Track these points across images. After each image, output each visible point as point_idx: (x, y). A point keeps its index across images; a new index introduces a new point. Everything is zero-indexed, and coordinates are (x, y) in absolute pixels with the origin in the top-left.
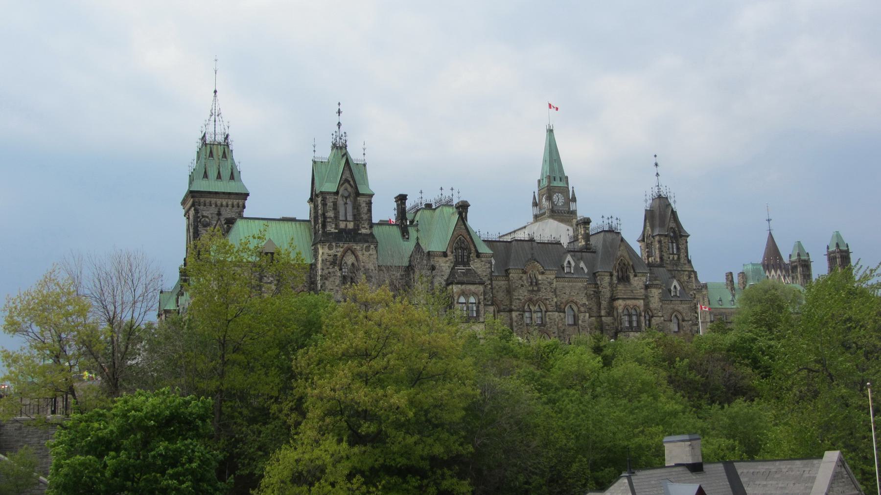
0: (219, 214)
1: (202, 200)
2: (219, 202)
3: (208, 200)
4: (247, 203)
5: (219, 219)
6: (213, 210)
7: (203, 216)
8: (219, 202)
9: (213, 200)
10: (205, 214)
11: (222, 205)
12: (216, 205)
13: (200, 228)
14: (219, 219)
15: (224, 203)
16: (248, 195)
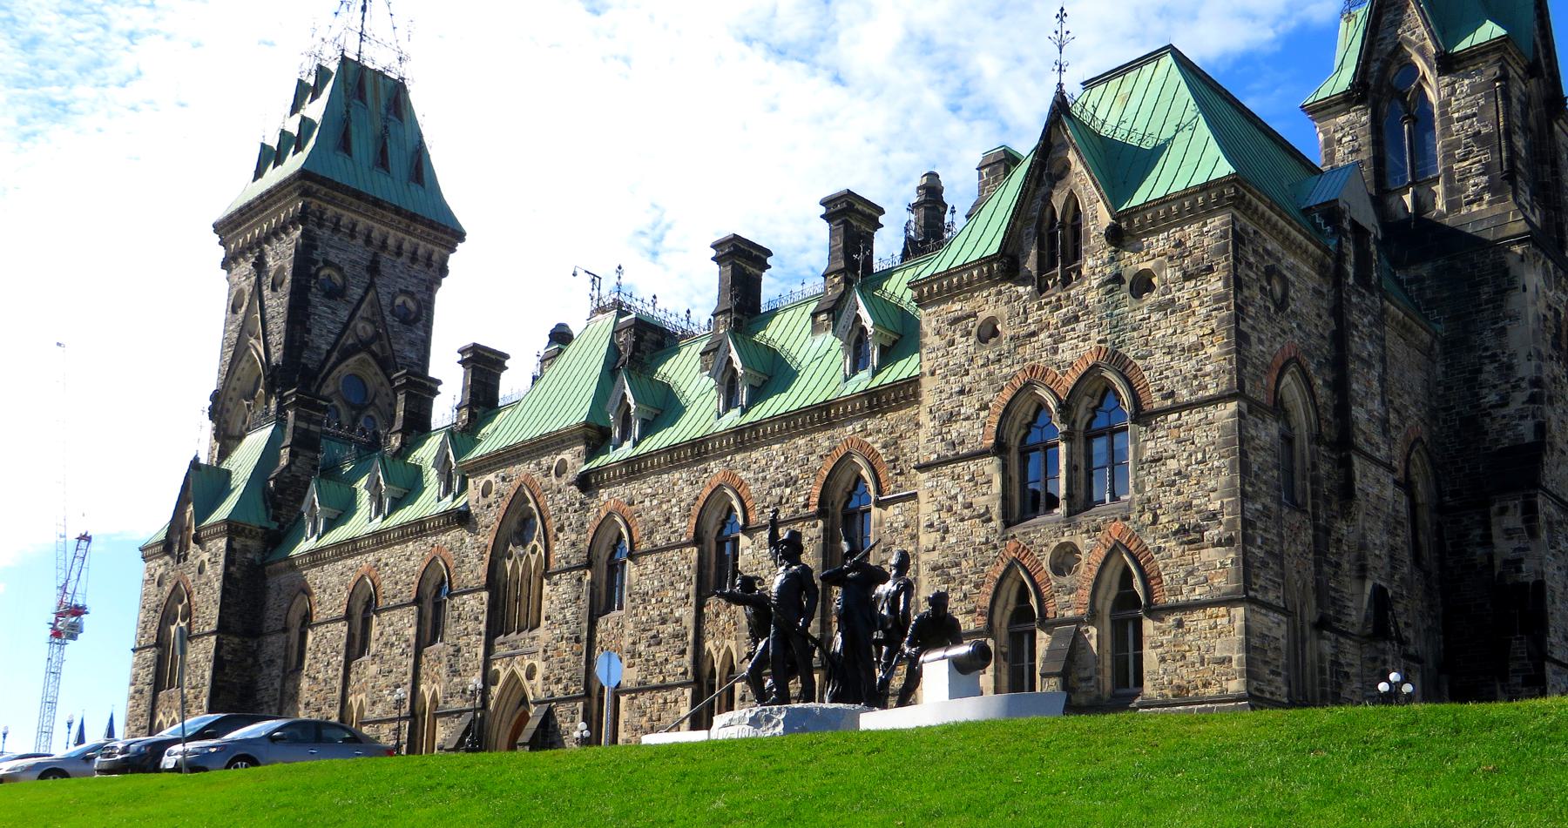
0: (374, 268)
1: (331, 210)
2: (378, 230)
3: (347, 217)
4: (453, 261)
5: (371, 286)
6: (358, 252)
7: (327, 263)
8: (378, 230)
9: (363, 223)
10: (333, 256)
11: (384, 246)
12: (368, 240)
13: (315, 298)
14: (371, 286)
15: (391, 242)
16: (460, 235)
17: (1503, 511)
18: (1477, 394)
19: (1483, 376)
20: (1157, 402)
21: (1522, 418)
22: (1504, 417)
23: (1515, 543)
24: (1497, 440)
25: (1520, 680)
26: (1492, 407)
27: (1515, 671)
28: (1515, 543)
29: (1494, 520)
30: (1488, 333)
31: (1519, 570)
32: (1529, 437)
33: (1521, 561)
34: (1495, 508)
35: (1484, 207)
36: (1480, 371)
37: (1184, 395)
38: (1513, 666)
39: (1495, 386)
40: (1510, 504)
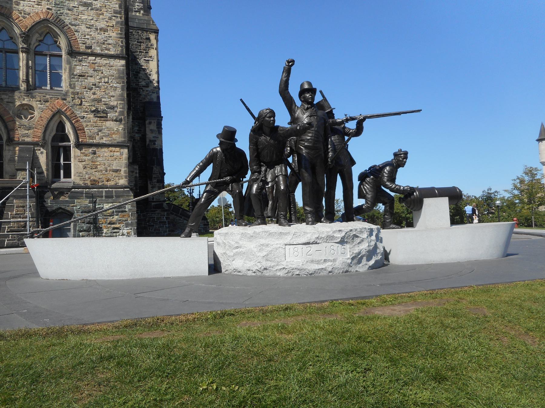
17: (150, 123)
18: (138, 81)
19: (140, 75)
20: (82, 48)
21: (153, 93)
22: (147, 91)
23: (154, 135)
24: (144, 98)
25: (156, 181)
26: (143, 86)
27: (155, 178)
28: (154, 135)
29: (147, 126)
30: (142, 60)
31: (154, 144)
32: (155, 100)
33: (155, 141)
34: (147, 122)
35: (141, 15)
36: (139, 73)
37: (98, 50)
38: (154, 176)
39: (145, 80)
40: (153, 121)
